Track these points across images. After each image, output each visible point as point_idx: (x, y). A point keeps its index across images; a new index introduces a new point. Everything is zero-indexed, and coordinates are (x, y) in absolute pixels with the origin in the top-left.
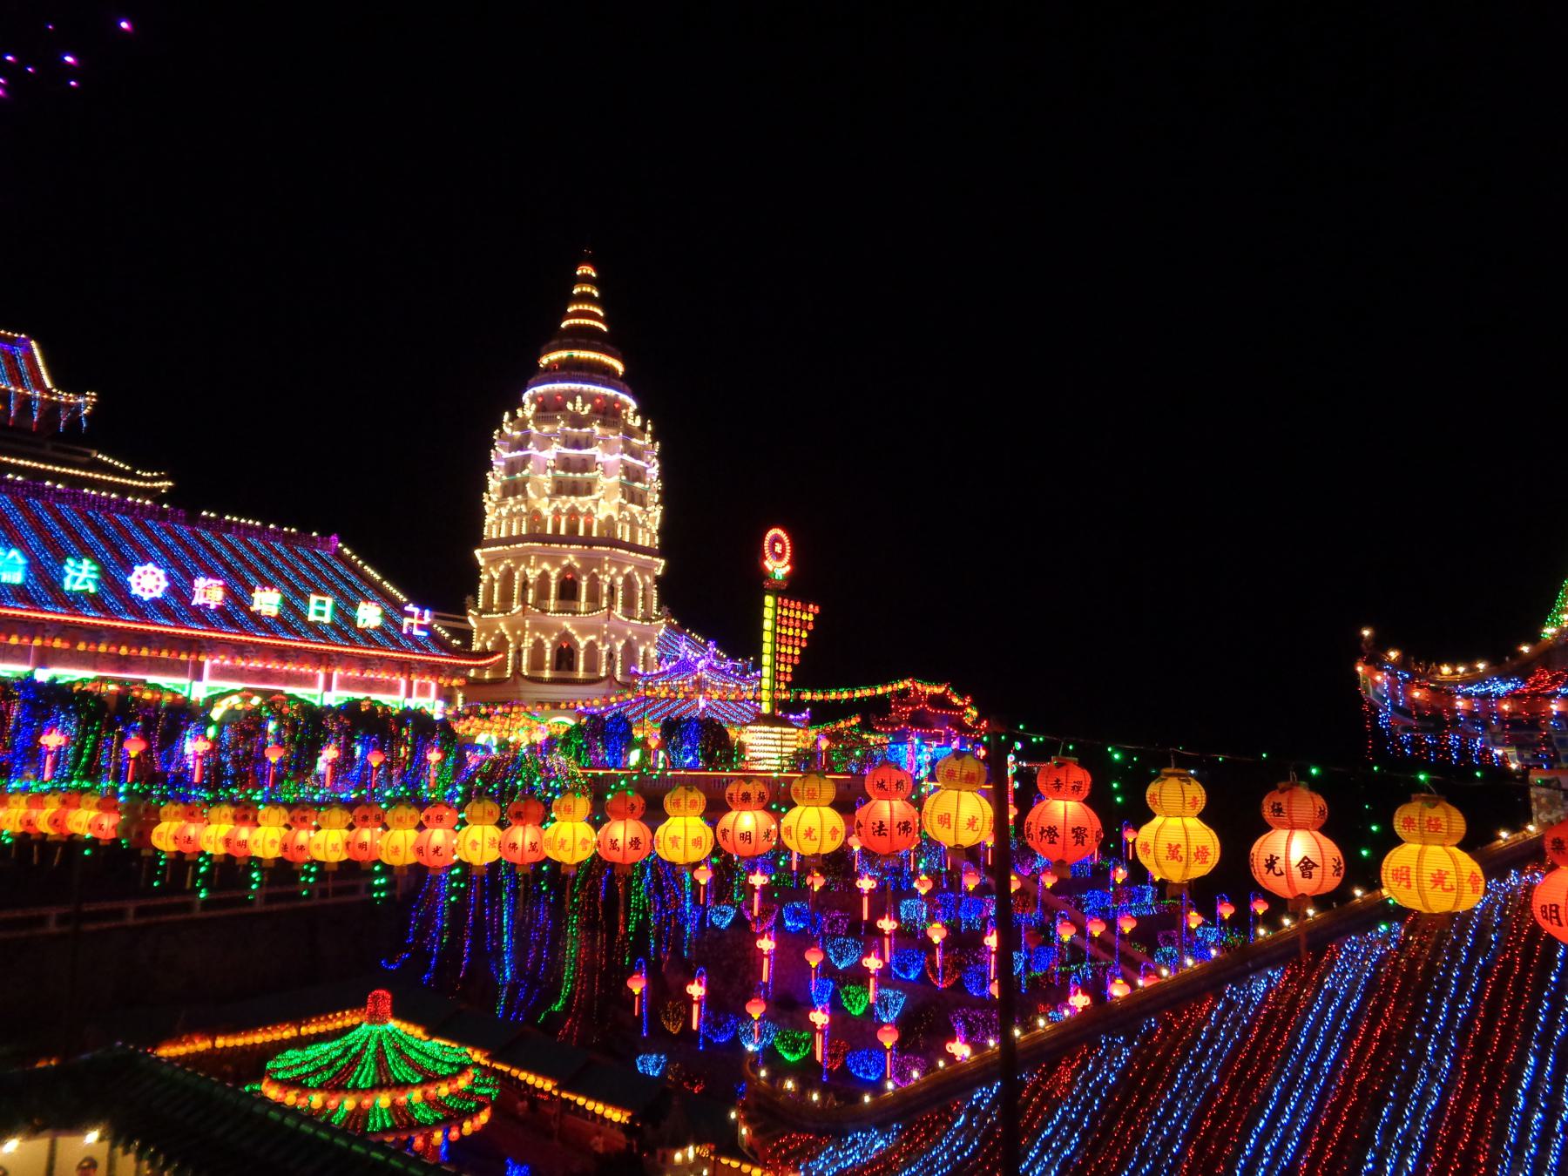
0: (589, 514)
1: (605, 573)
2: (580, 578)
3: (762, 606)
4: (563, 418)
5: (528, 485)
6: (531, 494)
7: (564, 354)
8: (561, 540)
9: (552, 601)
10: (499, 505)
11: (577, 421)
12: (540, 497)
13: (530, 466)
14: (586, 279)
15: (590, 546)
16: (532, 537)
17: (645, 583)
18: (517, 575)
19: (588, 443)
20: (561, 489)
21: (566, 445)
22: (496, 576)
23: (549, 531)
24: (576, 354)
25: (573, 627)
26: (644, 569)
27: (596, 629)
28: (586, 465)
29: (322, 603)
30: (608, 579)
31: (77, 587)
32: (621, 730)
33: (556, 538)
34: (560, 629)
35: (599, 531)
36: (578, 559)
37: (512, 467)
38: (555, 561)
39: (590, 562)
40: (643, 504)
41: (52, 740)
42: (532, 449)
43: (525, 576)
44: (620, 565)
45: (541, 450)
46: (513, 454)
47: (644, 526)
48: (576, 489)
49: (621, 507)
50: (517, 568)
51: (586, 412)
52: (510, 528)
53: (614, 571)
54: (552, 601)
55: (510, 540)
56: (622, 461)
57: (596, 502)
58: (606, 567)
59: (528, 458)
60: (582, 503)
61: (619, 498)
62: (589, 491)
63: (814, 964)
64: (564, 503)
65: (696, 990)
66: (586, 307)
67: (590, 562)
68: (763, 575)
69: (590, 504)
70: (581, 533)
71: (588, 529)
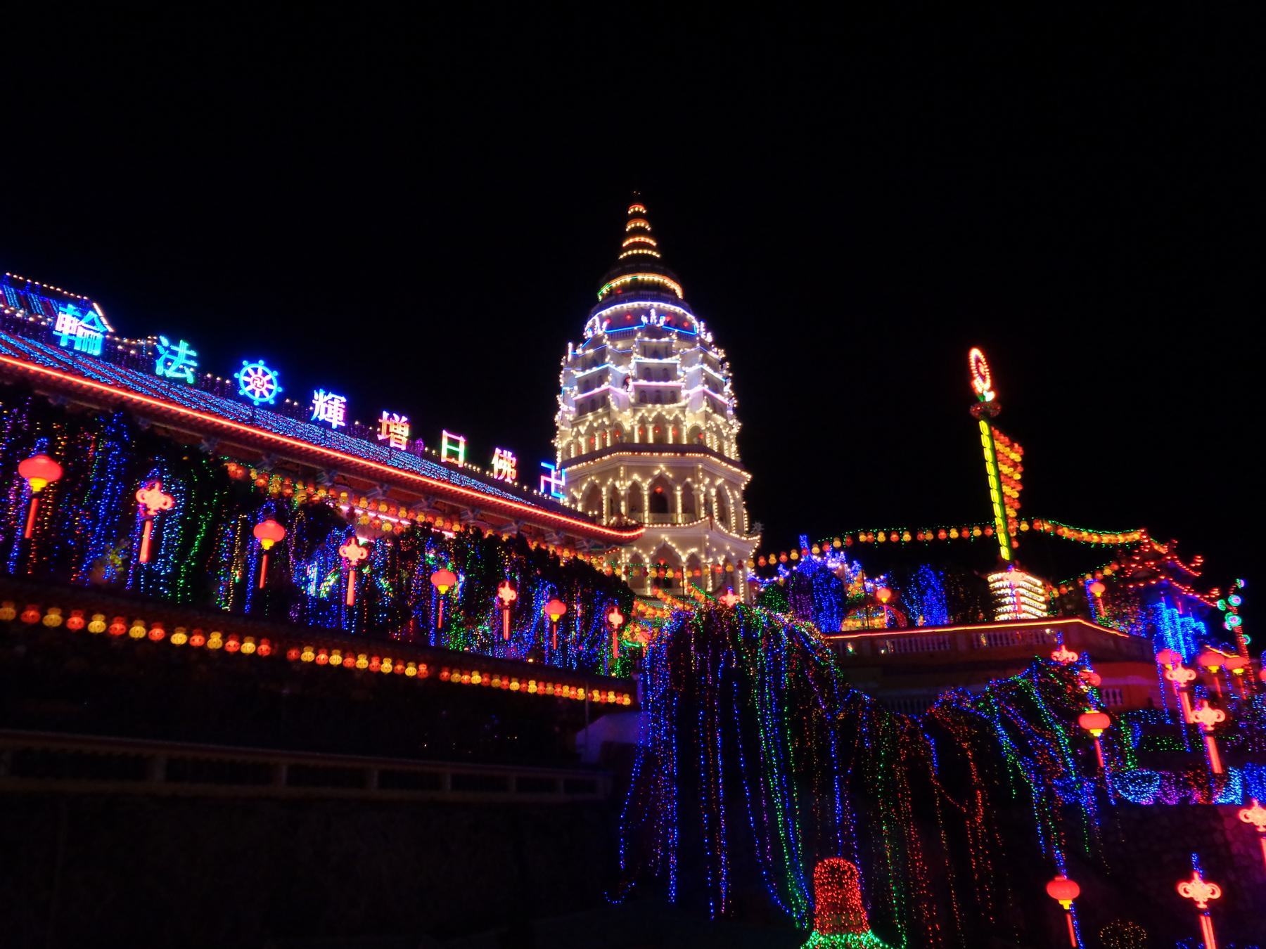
0: (677, 423)
1: (700, 482)
2: (672, 489)
3: (979, 433)
4: (640, 330)
5: (610, 397)
6: (614, 407)
7: (628, 279)
8: (651, 448)
9: (646, 514)
10: (574, 424)
11: (652, 331)
12: (622, 410)
13: (610, 378)
14: (637, 215)
15: (683, 453)
16: (619, 446)
17: (734, 496)
18: (604, 490)
19: (668, 353)
20: (645, 397)
22: (579, 496)
23: (637, 440)
24: (640, 277)
25: (672, 539)
26: (733, 484)
27: (698, 542)
28: (668, 373)
29: (456, 443)
30: (704, 489)
31: (171, 373)
32: (833, 585)
33: (644, 446)
34: (658, 542)
35: (688, 439)
36: (670, 468)
37: (586, 385)
38: (645, 472)
39: (683, 471)
40: (723, 413)
41: (154, 499)
42: (609, 363)
43: (614, 490)
44: (713, 477)
45: (618, 365)
46: (588, 372)
47: (727, 438)
48: (660, 397)
49: (707, 417)
50: (603, 483)
51: (662, 323)
52: (591, 444)
53: (707, 481)
54: (646, 514)
55: (592, 455)
56: (703, 370)
57: (683, 409)
58: (701, 475)
59: (606, 371)
60: (668, 410)
61: (704, 407)
62: (673, 396)
63: (1066, 904)
64: (650, 411)
65: (1199, 891)
66: (642, 239)
67: (683, 471)
68: (973, 398)
69: (677, 412)
70: (671, 441)
71: (677, 437)
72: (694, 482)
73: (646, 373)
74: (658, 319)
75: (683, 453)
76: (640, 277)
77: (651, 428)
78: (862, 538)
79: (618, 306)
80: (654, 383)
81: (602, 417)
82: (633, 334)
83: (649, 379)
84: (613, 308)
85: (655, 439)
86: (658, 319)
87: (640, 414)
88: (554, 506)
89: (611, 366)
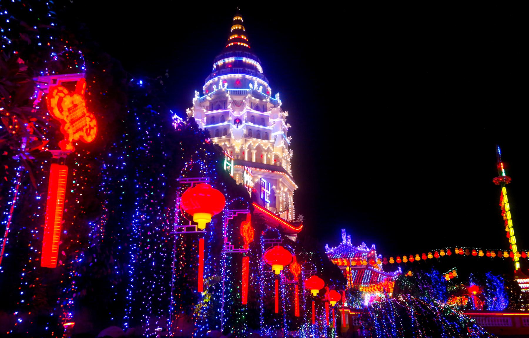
14: (238, 22)
21: (252, 107)
24: (244, 59)
48: (259, 135)
64: (254, 143)
69: (269, 145)
72: (277, 189)
73: (252, 119)
74: (259, 87)
75: (273, 171)
76: (244, 59)
77: (254, 153)
78: (457, 251)
79: (233, 75)
80: (257, 126)
81: (224, 141)
82: (246, 93)
83: (255, 123)
84: (229, 75)
85: (256, 159)
86: (259, 87)
87: (249, 143)
88: (266, 210)
89: (231, 111)
